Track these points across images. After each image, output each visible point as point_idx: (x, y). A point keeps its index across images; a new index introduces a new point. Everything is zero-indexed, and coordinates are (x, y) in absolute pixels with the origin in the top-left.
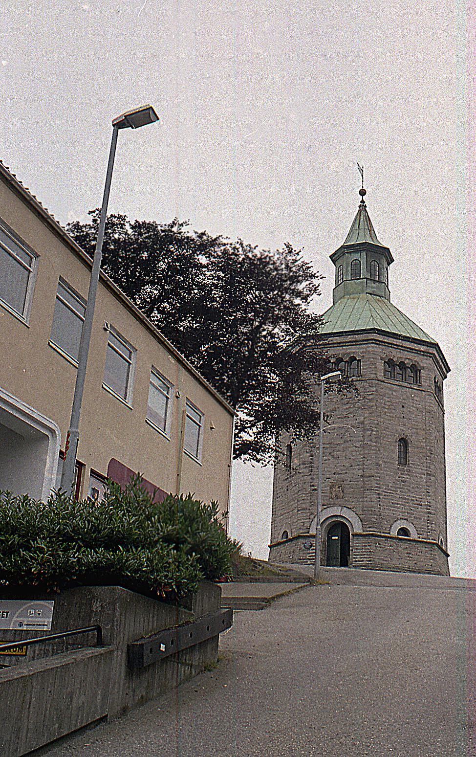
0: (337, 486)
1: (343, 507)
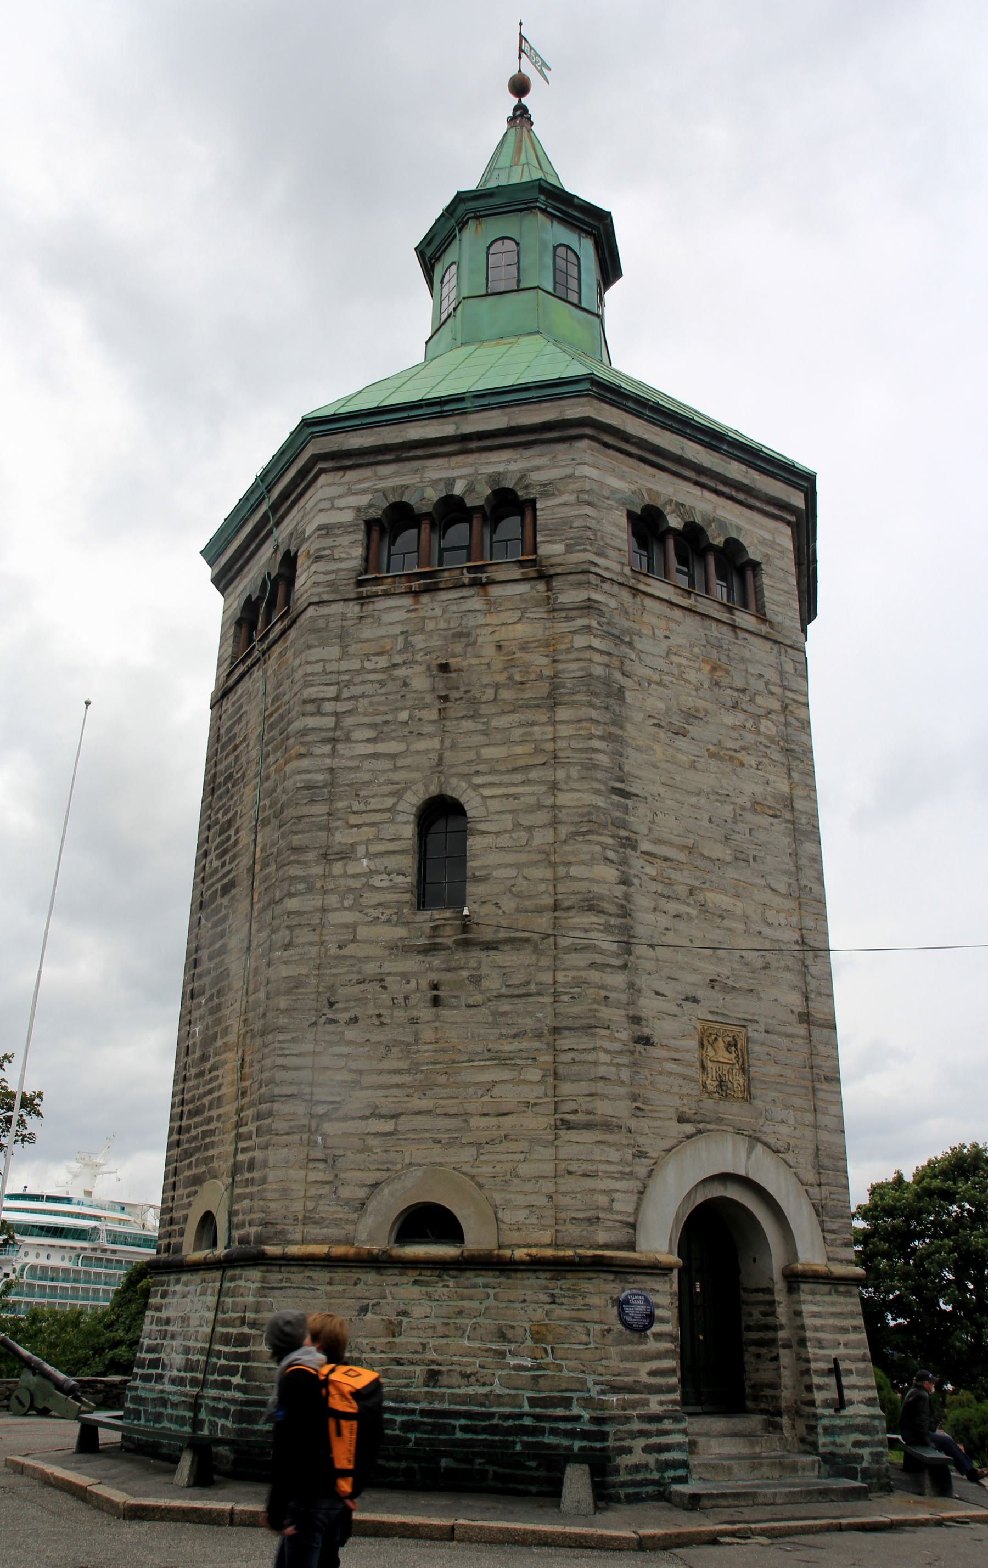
1: (754, 1139)
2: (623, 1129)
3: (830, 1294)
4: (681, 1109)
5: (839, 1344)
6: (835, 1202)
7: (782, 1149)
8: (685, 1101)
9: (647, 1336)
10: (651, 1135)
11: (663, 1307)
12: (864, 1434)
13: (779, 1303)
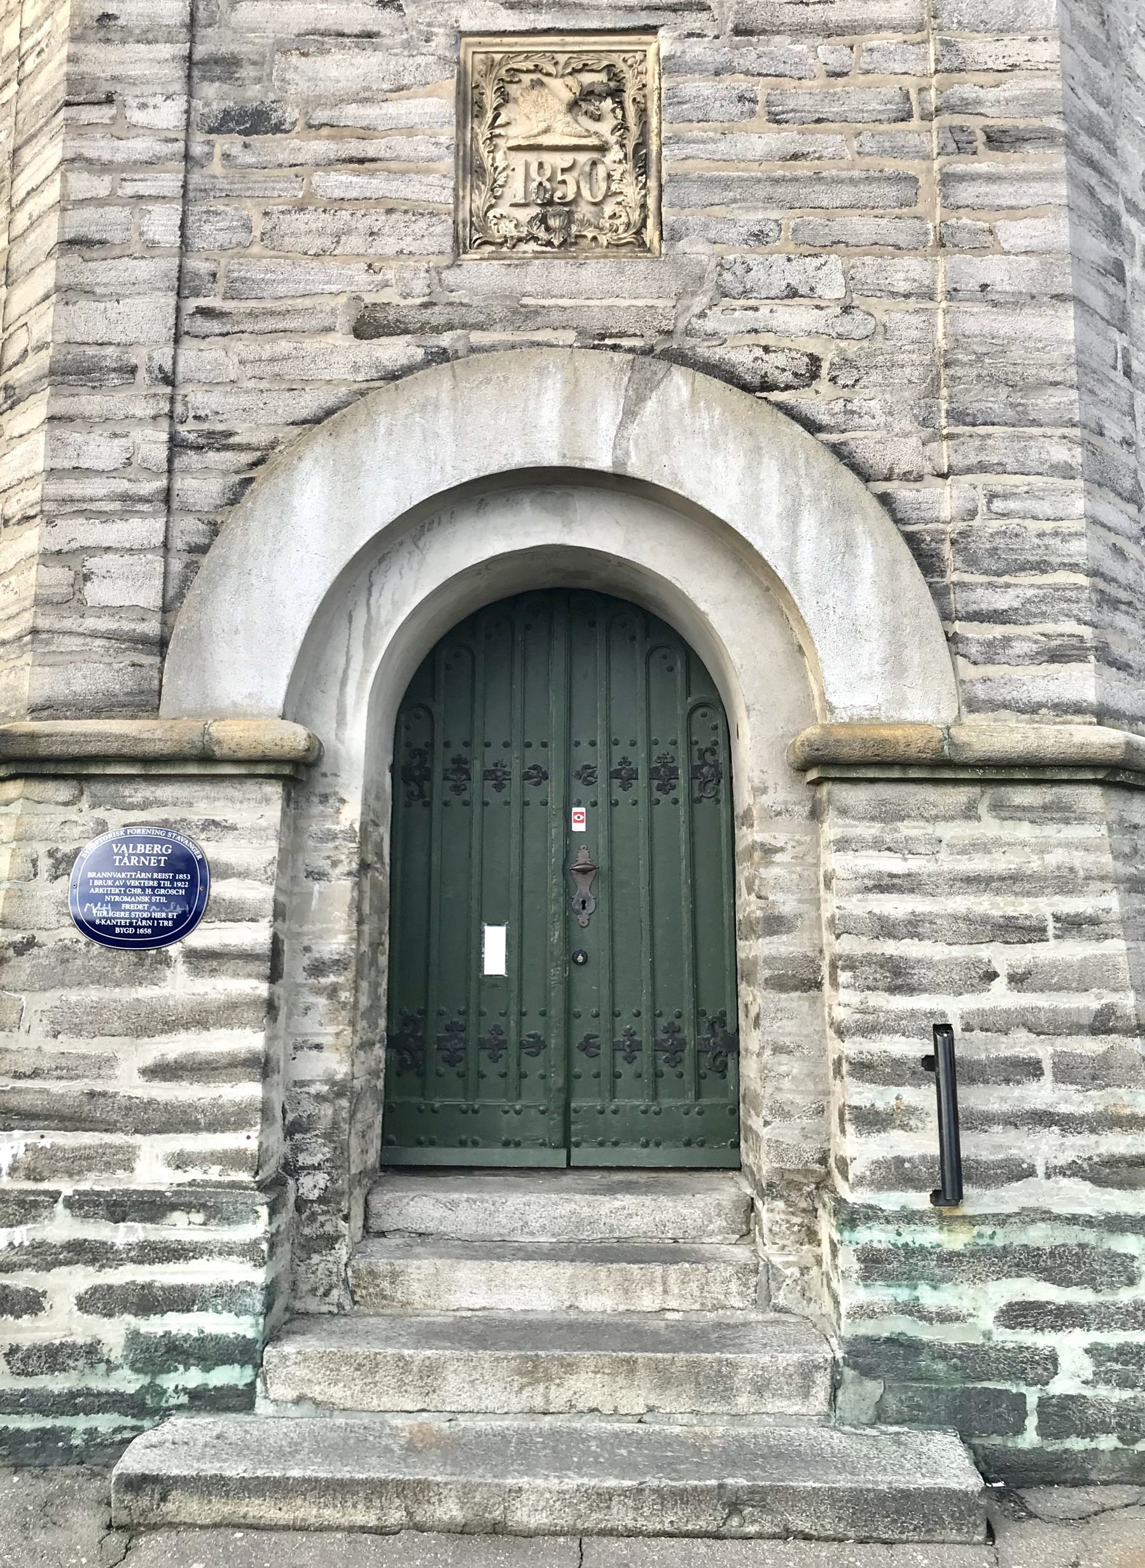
0: (561, 90)
2: (142, 374)
3: (969, 813)
4: (369, 299)
5: (992, 976)
6: (1013, 524)
7: (787, 378)
8: (390, 275)
9: (167, 961)
10: (251, 384)
11: (244, 874)
12: (1064, 1282)
13: (769, 851)
